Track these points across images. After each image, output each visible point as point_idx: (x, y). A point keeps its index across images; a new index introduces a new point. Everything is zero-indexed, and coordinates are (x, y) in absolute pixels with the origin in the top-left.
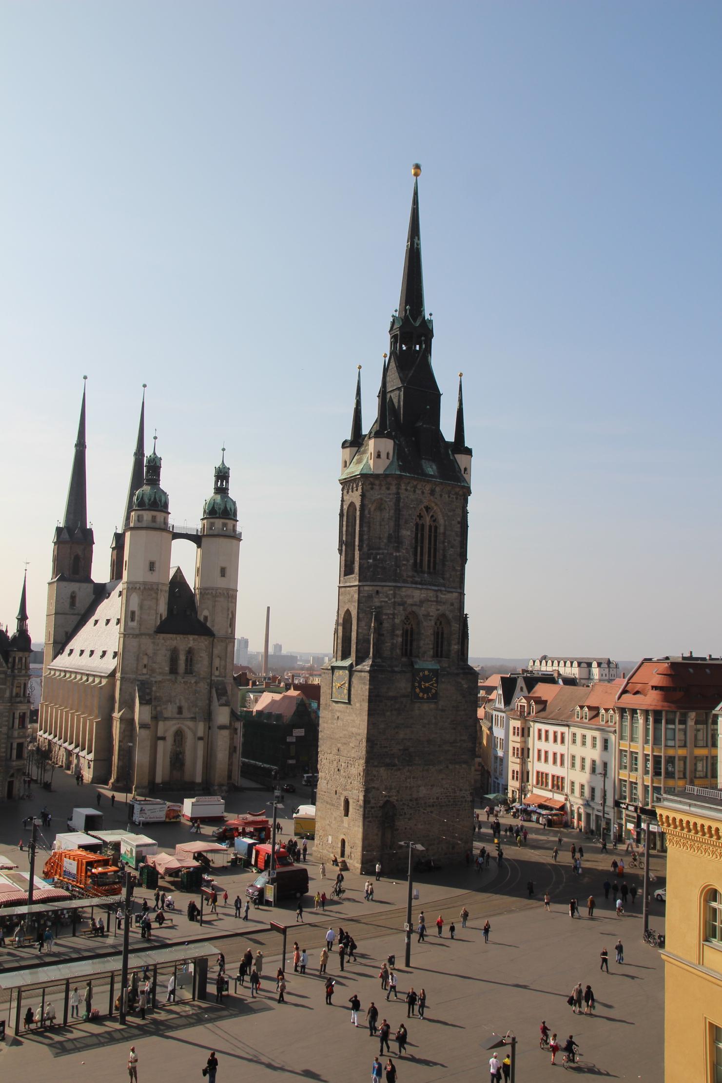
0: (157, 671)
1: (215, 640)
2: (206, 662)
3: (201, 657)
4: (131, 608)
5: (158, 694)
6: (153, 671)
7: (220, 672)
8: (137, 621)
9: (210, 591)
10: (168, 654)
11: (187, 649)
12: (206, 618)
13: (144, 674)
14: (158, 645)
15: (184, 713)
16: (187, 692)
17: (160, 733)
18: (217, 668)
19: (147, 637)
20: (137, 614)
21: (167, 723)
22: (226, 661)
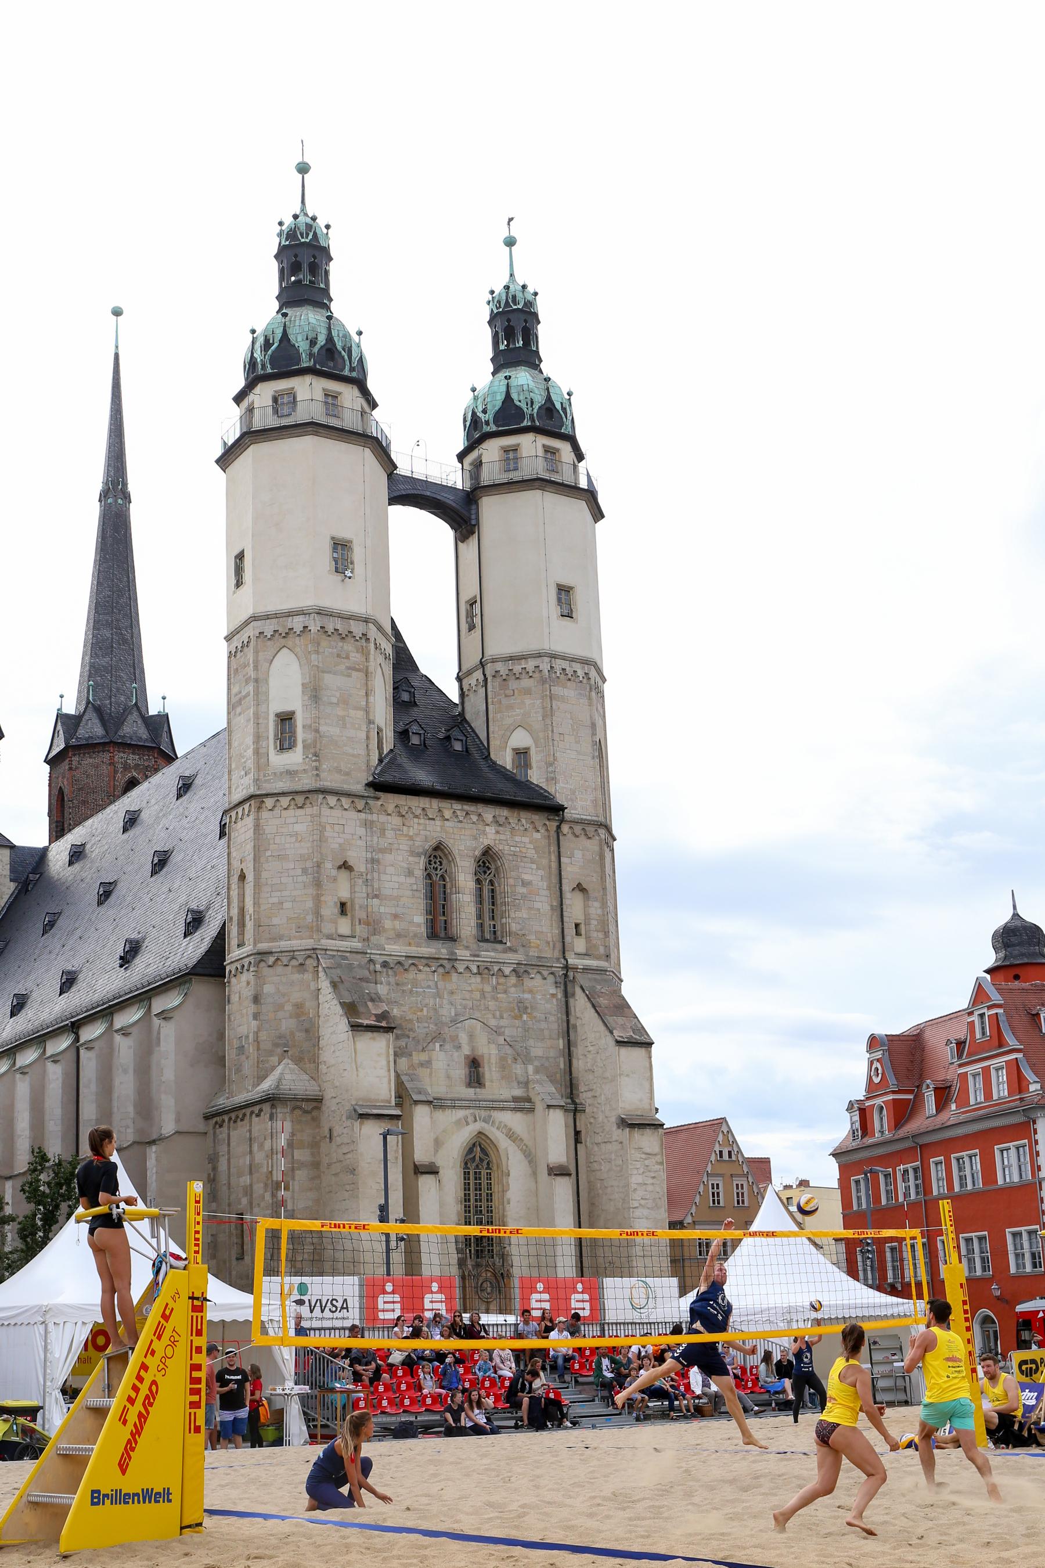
0: (388, 924)
1: (565, 828)
2: (543, 903)
3: (524, 884)
4: (277, 706)
6: (373, 925)
7: (588, 938)
8: (304, 747)
9: (531, 665)
11: (478, 853)
12: (522, 754)
13: (342, 937)
14: (383, 831)
15: (487, 1084)
16: (492, 1004)
17: (421, 1155)
18: (577, 926)
19: (346, 802)
20: (300, 721)
21: (439, 1115)
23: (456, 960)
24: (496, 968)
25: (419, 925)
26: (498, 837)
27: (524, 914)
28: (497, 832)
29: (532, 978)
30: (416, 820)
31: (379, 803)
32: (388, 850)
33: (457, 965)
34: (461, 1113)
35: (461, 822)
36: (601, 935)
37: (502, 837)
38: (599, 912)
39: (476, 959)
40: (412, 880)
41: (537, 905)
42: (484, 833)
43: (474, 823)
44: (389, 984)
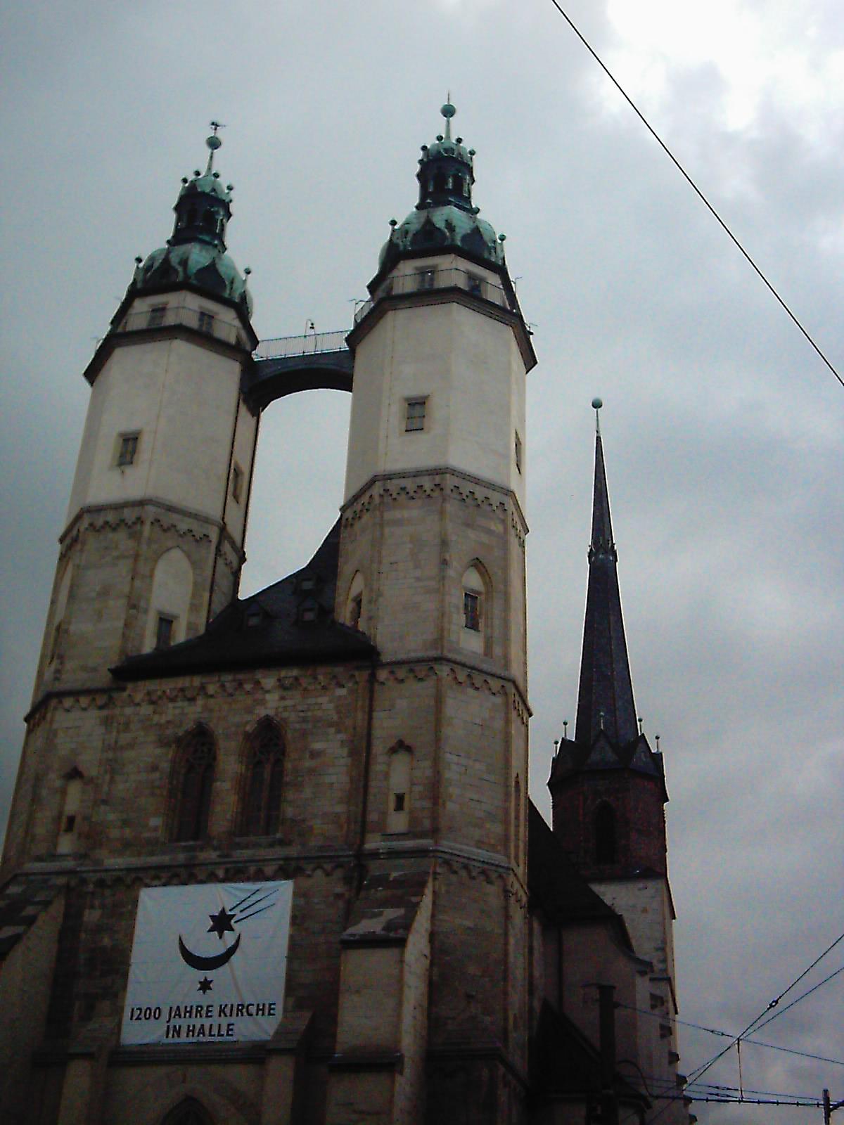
0: (115, 833)
1: (383, 675)
2: (338, 774)
3: (314, 755)
5: (106, 941)
6: (93, 837)
10: (165, 757)
18: (400, 799)
19: (84, 701)
22: (436, 762)
23: (195, 865)
24: (252, 869)
25: (156, 829)
26: (284, 703)
27: (307, 792)
28: (283, 698)
29: (309, 876)
30: (171, 705)
31: (125, 694)
32: (131, 746)
33: (196, 871)
34: (161, 1071)
35: (231, 695)
36: (427, 804)
37: (289, 703)
38: (429, 772)
39: (226, 860)
40: (157, 775)
41: (327, 779)
42: (263, 702)
43: (248, 693)
44: (103, 906)
